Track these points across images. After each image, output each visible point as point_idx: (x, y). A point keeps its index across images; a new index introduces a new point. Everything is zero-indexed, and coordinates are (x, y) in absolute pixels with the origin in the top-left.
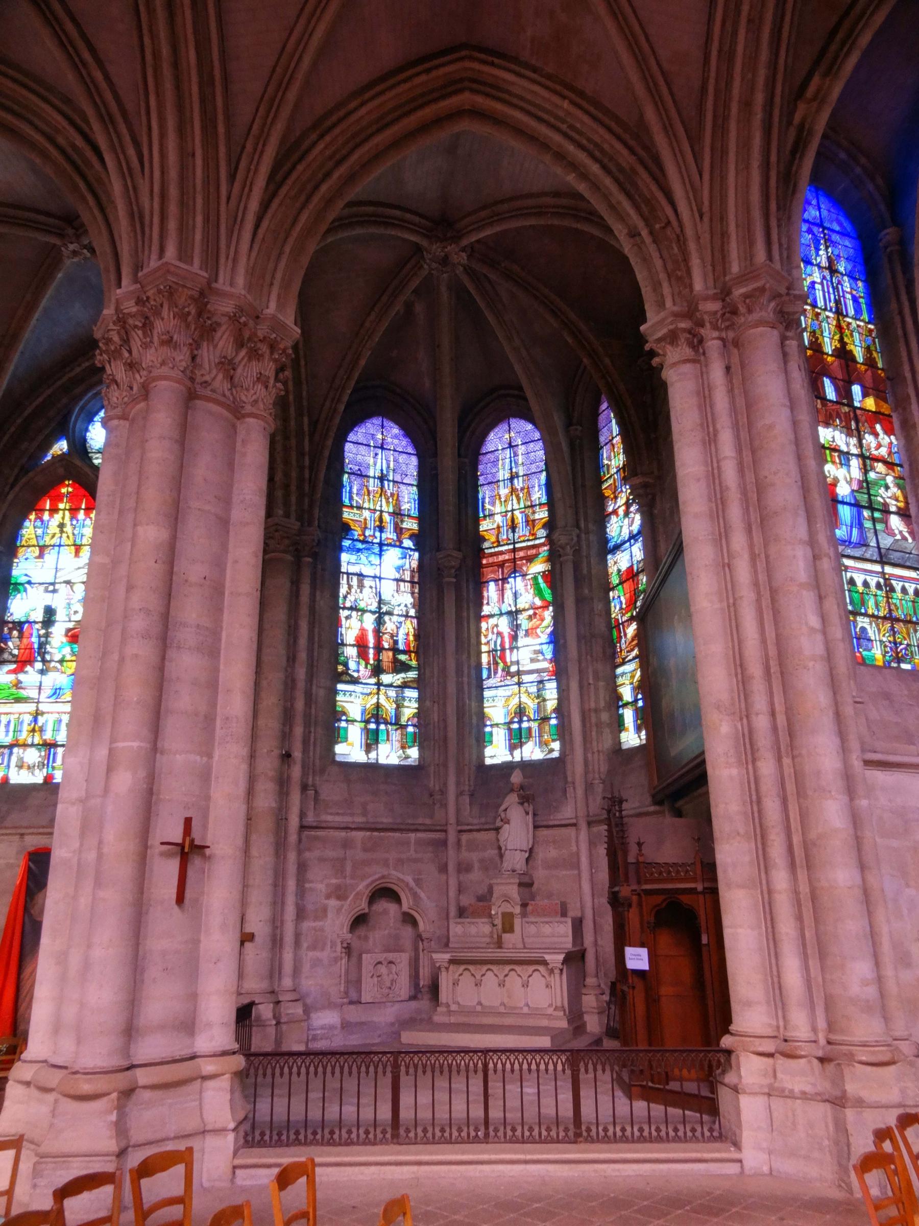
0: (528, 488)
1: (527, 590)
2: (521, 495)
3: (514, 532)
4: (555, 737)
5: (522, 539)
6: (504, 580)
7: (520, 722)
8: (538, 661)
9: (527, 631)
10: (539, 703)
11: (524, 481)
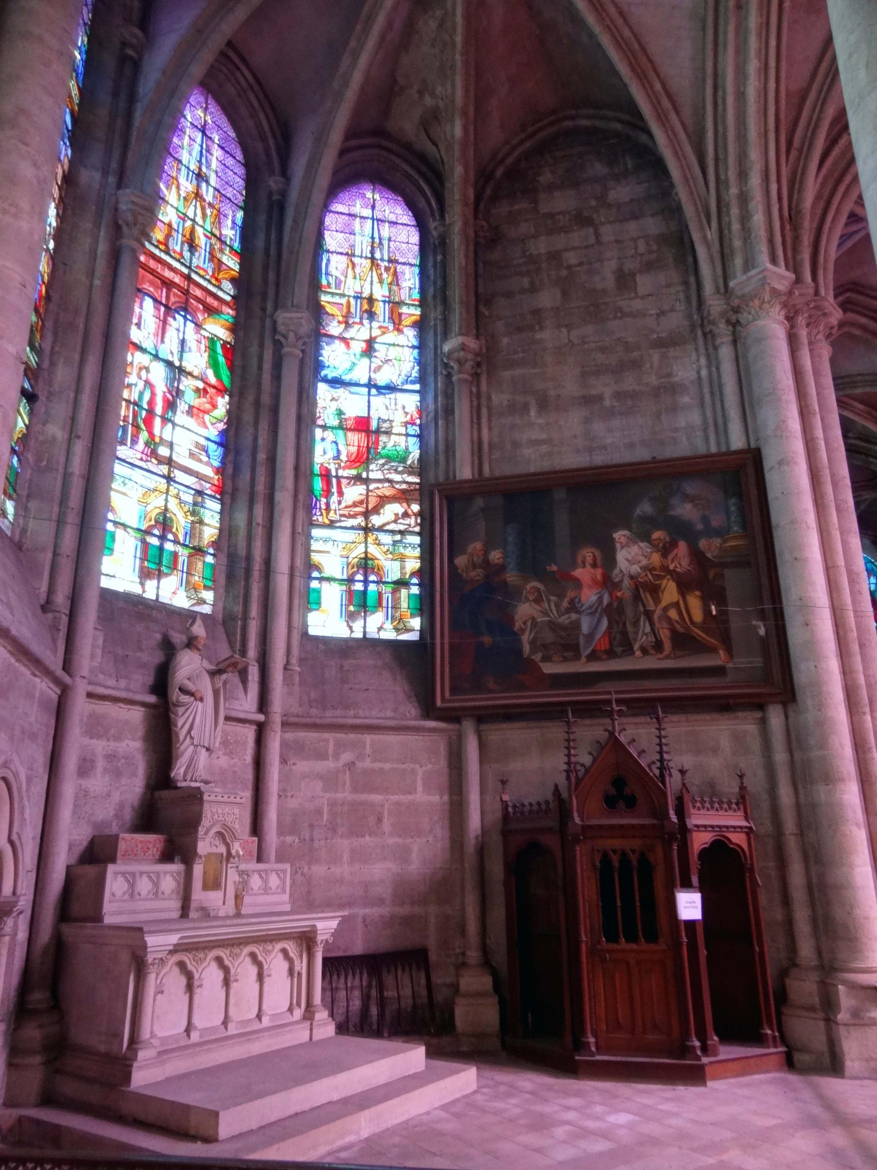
1: (199, 350)
4: (209, 583)
7: (163, 538)
8: (200, 461)
9: (191, 407)
10: (193, 522)
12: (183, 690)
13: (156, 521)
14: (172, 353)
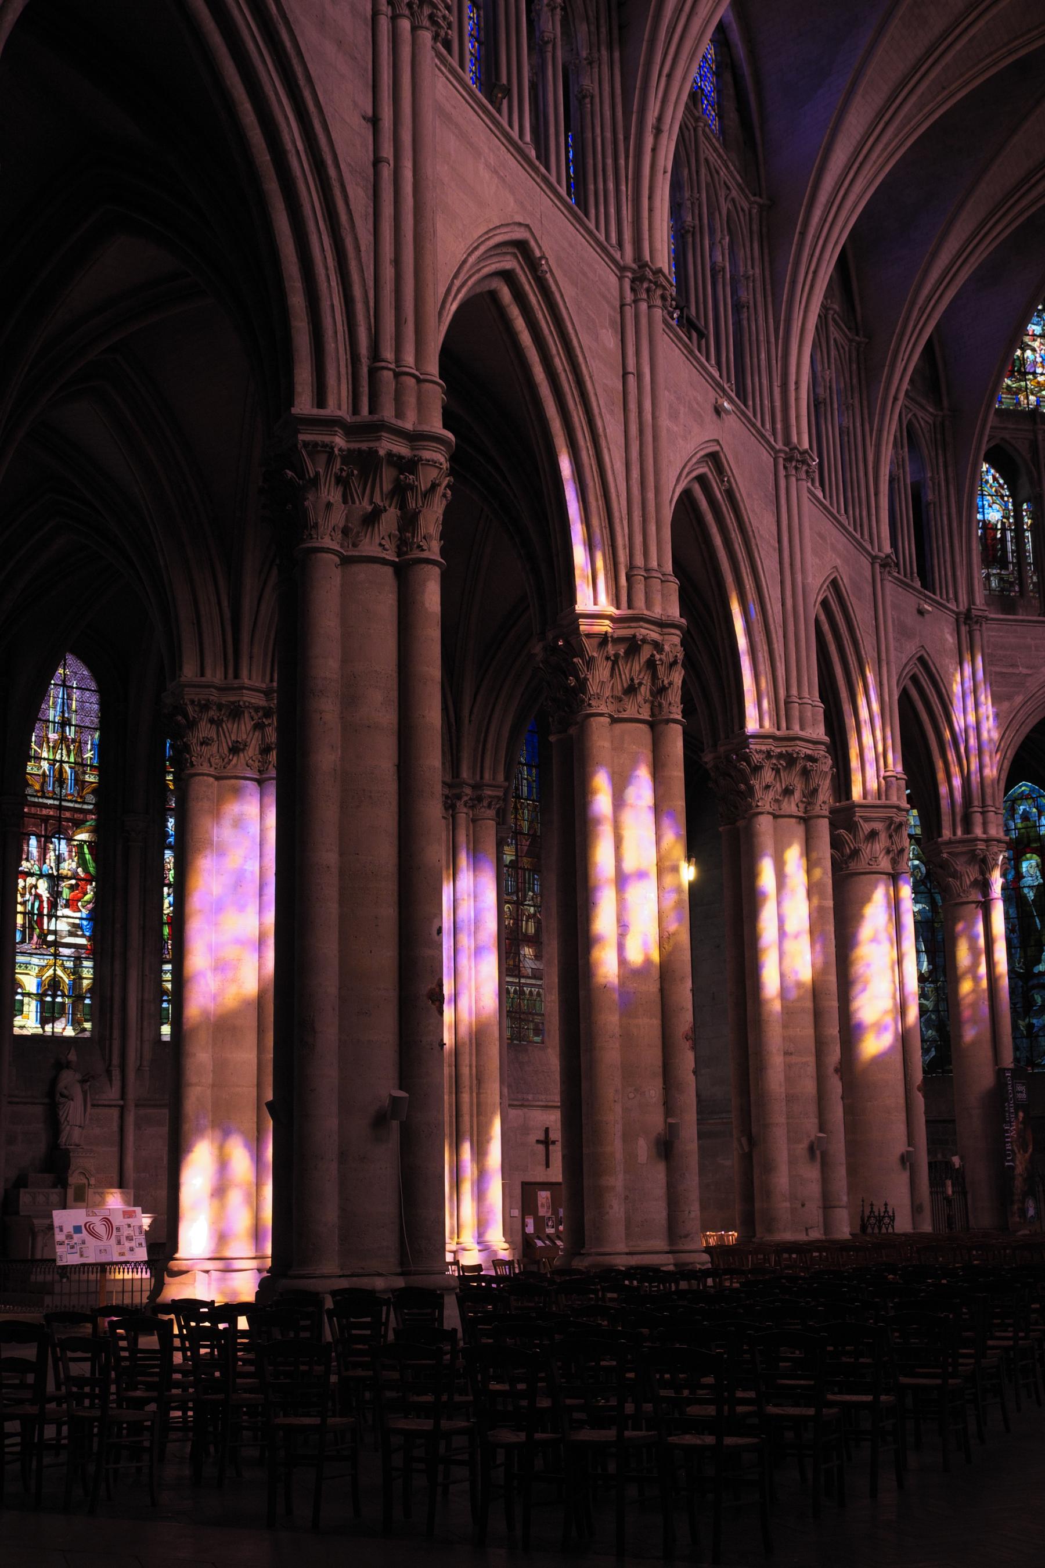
0: (80, 742)
1: (71, 857)
2: (72, 747)
3: (61, 787)
4: (88, 1017)
5: (70, 798)
6: (48, 839)
7: (54, 996)
8: (77, 936)
9: (67, 901)
11: (76, 732)
12: (62, 1095)
13: (49, 985)
14: (51, 868)
